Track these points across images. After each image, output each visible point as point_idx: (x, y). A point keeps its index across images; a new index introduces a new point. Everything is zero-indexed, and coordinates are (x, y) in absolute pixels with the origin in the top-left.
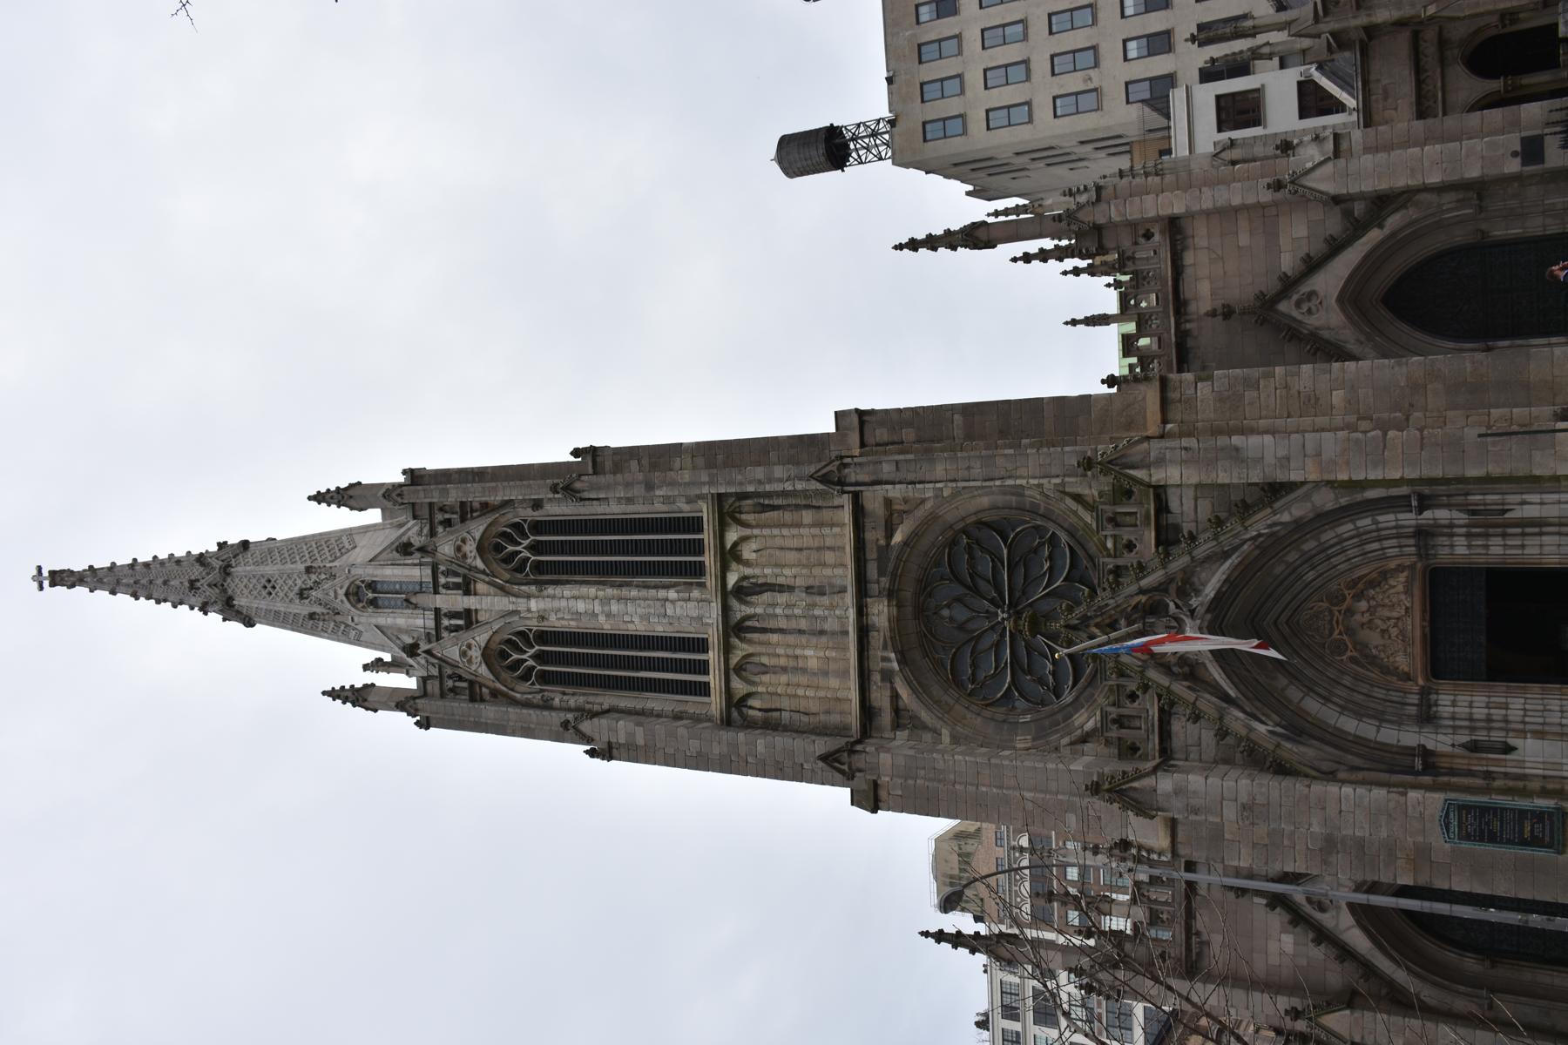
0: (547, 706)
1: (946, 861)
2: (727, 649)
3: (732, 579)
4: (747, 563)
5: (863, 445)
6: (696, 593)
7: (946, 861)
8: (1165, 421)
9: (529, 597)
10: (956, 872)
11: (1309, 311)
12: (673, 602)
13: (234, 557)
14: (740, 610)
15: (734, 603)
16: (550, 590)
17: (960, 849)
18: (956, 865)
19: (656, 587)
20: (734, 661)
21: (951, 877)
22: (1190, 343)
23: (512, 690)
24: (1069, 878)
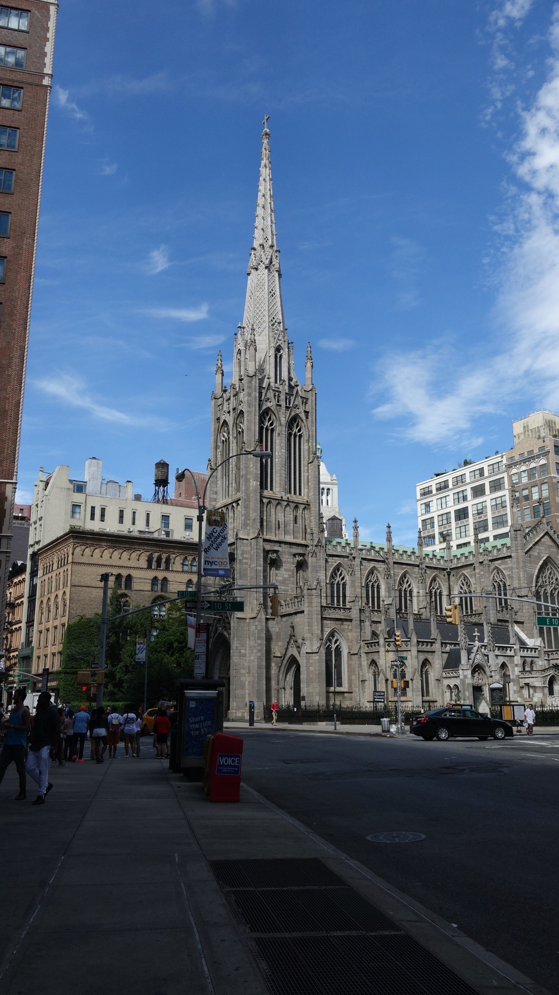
0: (216, 447)
1: (534, 421)
2: (224, 506)
3: (234, 504)
4: (237, 508)
5: (251, 539)
6: (234, 492)
7: (534, 421)
8: (251, 618)
9: (233, 435)
10: (530, 428)
11: (292, 647)
12: (232, 486)
13: (263, 264)
14: (230, 507)
15: (231, 505)
16: (235, 441)
17: (541, 427)
18: (533, 427)
19: (236, 478)
20: (223, 509)
21: (528, 426)
22: (291, 616)
23: (220, 433)
24: (532, 489)
